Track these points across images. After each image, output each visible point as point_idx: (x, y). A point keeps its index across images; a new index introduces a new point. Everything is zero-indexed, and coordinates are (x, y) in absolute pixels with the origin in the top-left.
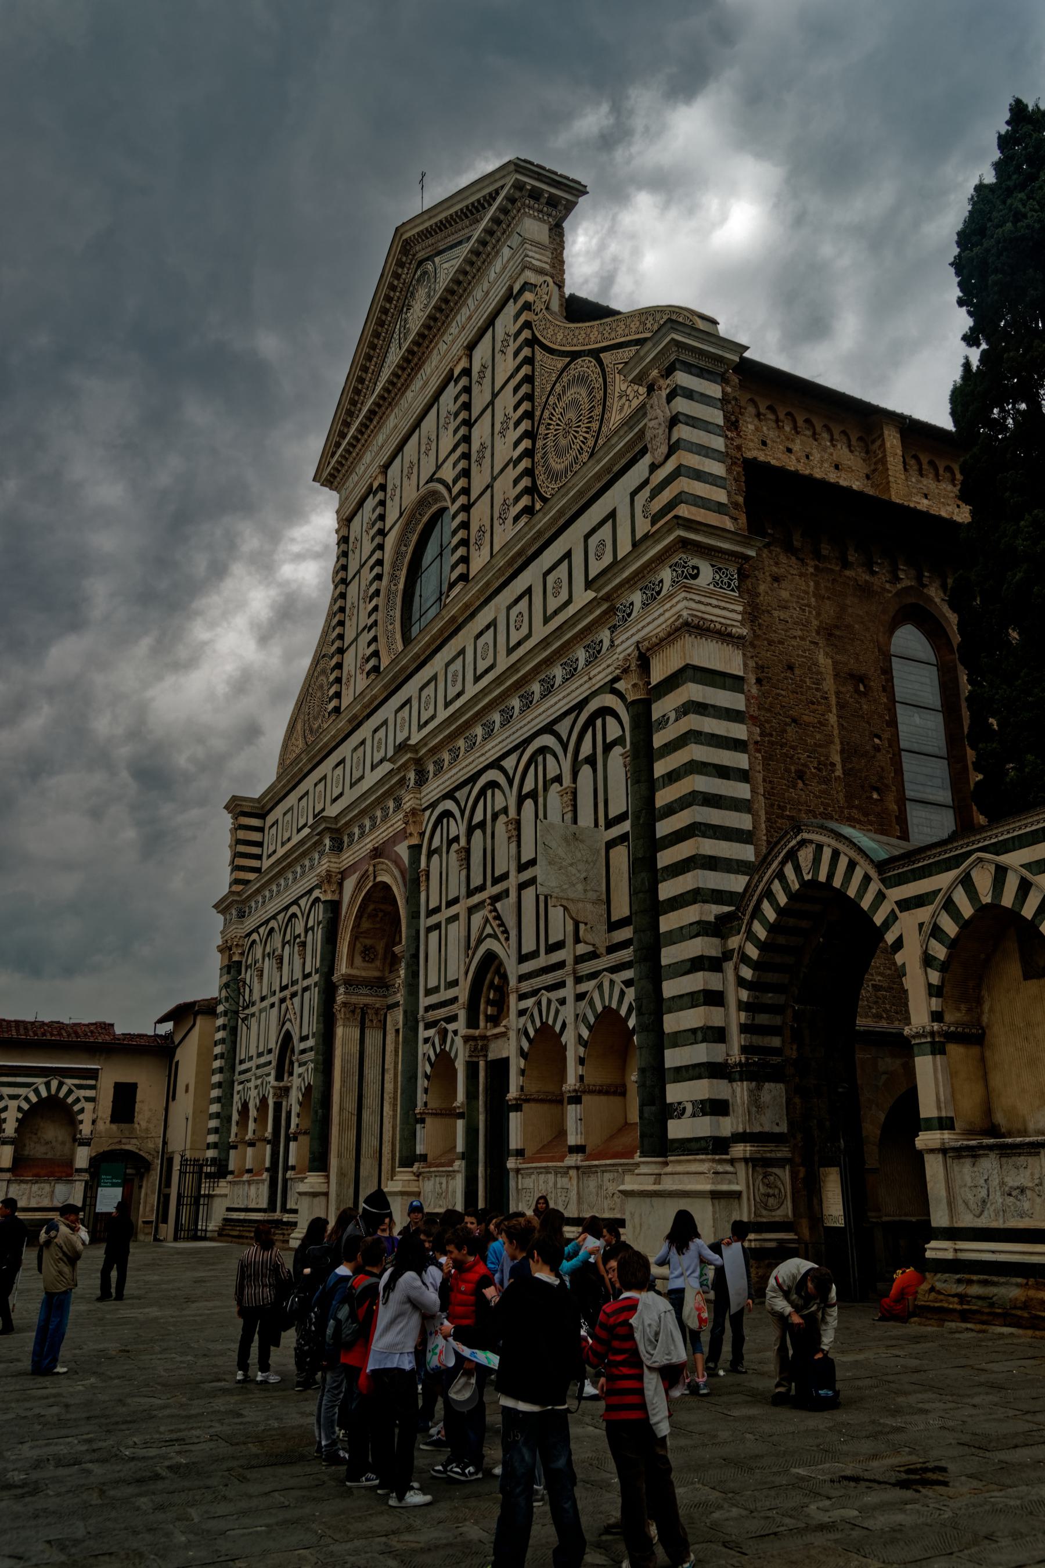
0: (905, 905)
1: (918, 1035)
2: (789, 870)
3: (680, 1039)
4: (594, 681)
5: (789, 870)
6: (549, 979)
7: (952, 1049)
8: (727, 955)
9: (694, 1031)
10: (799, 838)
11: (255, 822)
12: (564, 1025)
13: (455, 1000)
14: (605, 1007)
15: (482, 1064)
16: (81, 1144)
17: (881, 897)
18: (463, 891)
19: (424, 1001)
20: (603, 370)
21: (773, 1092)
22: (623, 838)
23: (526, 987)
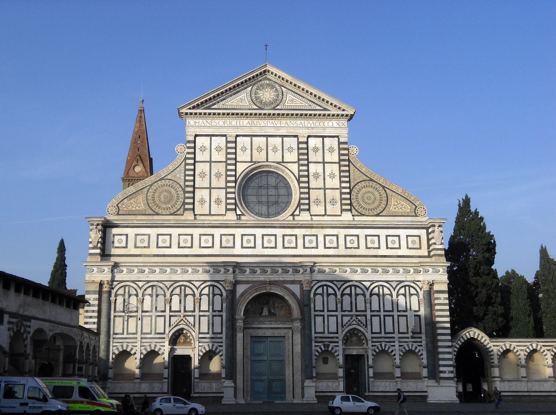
0: (494, 346)
2: (467, 334)
3: (443, 359)
13: (337, 338)
14: (409, 349)
16: (90, 365)
17: (488, 343)
18: (339, 309)
19: (314, 335)
20: (386, 193)
23: (374, 340)
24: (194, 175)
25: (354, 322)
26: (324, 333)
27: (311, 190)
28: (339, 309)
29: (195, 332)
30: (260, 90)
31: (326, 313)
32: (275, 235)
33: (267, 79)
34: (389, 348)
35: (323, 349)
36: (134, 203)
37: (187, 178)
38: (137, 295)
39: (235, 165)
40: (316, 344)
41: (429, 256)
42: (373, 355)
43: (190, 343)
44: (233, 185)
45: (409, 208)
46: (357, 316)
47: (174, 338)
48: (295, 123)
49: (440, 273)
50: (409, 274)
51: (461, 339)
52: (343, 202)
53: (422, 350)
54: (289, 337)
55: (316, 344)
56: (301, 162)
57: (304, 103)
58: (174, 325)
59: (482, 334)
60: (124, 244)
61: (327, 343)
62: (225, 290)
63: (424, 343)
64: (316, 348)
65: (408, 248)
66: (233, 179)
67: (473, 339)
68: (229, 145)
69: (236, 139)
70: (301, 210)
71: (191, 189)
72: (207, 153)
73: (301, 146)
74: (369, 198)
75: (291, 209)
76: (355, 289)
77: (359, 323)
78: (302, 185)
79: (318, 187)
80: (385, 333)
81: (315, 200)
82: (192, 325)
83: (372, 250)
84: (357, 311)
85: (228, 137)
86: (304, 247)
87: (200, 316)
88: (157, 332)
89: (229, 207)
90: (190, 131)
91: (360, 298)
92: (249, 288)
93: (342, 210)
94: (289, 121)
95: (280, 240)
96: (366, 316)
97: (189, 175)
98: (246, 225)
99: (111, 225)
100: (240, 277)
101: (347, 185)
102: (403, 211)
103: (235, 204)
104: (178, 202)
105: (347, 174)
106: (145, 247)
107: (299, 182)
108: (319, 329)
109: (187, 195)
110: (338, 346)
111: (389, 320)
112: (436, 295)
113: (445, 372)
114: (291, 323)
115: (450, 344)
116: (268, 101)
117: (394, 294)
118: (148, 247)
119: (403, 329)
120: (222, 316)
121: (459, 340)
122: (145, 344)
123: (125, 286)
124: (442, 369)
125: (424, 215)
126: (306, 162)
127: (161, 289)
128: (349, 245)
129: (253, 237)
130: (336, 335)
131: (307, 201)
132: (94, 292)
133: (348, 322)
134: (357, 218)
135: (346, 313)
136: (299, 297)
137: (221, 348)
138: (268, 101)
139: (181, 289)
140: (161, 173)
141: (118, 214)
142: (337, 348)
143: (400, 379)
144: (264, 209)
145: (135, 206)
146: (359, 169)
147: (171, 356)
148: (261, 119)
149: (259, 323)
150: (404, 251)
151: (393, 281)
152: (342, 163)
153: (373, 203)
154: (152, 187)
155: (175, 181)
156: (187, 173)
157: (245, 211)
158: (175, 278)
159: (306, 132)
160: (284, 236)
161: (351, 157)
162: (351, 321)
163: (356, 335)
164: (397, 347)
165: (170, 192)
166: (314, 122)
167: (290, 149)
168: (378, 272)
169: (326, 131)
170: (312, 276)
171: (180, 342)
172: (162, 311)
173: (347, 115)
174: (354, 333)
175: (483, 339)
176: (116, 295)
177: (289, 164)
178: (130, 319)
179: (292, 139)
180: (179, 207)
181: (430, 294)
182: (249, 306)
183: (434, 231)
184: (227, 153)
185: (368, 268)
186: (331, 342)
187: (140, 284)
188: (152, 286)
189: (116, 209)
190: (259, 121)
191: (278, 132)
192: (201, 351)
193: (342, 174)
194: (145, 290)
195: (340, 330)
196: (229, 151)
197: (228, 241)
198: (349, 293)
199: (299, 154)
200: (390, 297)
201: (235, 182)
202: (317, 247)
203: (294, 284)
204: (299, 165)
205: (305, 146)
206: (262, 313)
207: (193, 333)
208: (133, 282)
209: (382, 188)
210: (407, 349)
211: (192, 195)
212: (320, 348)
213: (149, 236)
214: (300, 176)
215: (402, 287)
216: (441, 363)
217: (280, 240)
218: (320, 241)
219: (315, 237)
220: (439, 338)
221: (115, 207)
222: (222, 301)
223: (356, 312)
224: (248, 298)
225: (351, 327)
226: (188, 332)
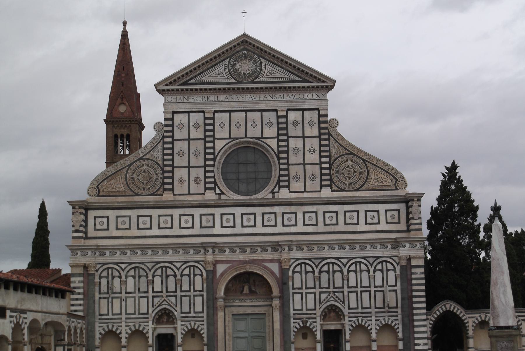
0: (469, 317)
1: (470, 336)
2: (443, 307)
4: (385, 254)
5: (443, 307)
6: (364, 315)
8: (427, 319)
10: (447, 303)
11: (84, 211)
13: (315, 314)
15: (322, 330)
17: (464, 315)
18: (317, 286)
19: (292, 312)
22: (394, 291)
23: (351, 315)
24: (172, 154)
25: (332, 299)
26: (302, 310)
27: (291, 167)
28: (317, 286)
29: (177, 312)
30: (238, 62)
31: (304, 291)
32: (255, 214)
33: (245, 49)
34: (366, 323)
35: (302, 325)
36: (113, 184)
37: (166, 157)
38: (120, 277)
39: (214, 142)
40: (295, 321)
41: (408, 231)
42: (350, 330)
43: (173, 323)
44: (212, 163)
45: (390, 181)
46: (334, 292)
48: (273, 96)
49: (417, 248)
50: (386, 249)
52: (323, 177)
53: (398, 324)
54: (269, 315)
55: (295, 321)
56: (281, 137)
57: (283, 74)
58: (157, 305)
59: (458, 307)
60: (105, 226)
61: (305, 319)
62: (206, 270)
63: (400, 317)
64: (294, 325)
65: (387, 223)
66: (212, 157)
67: (448, 312)
68: (207, 122)
69: (214, 114)
70: (280, 187)
71: (170, 169)
72: (185, 130)
73: (280, 120)
74: (349, 172)
75: (270, 186)
76: (333, 266)
77: (337, 299)
78: (281, 161)
79: (298, 163)
80: (362, 308)
81: (294, 177)
82: (174, 305)
83: (351, 226)
84: (334, 287)
85: (206, 114)
86: (284, 225)
87: (182, 296)
88: (141, 312)
89: (208, 186)
90: (167, 108)
91: (338, 275)
92: (229, 268)
93: (322, 186)
94: (268, 94)
95: (259, 219)
96: (343, 292)
97: (167, 154)
98: (225, 204)
99: (92, 207)
100: (220, 257)
101: (327, 160)
102: (384, 185)
104: (157, 182)
105: (327, 148)
106: (126, 229)
107: (279, 158)
108: (298, 306)
109: (166, 175)
110: (316, 322)
111: (366, 296)
112: (413, 270)
113: (419, 344)
114: (271, 300)
115: (425, 317)
116: (246, 73)
117: (372, 270)
118: (130, 228)
119: (379, 304)
120: (202, 296)
121: (435, 313)
122: (130, 324)
123: (108, 268)
124: (417, 341)
126: (285, 137)
127: (143, 271)
128: (328, 222)
129: (232, 216)
130: (314, 312)
131: (286, 178)
132: (79, 275)
133: (326, 299)
134: (336, 194)
135: (324, 290)
136: (278, 275)
137: (202, 326)
138: (246, 73)
139: (162, 270)
140: (140, 152)
141: (98, 196)
142: (315, 324)
144: (243, 187)
145: (115, 187)
146: (340, 142)
147: (155, 334)
148: (239, 93)
149: (241, 301)
150: (383, 226)
152: (323, 137)
153: (354, 177)
154: (131, 167)
155: (153, 161)
156: (166, 152)
157: (225, 189)
158: (156, 259)
159: (285, 106)
160: (263, 214)
161: (332, 130)
162: (329, 297)
163: (334, 311)
164: (374, 322)
165: (149, 172)
166: (294, 94)
167: (270, 124)
168: (355, 249)
169: (306, 103)
170: (290, 254)
171: (163, 321)
172: (145, 292)
173: (327, 87)
174: (332, 309)
175: (459, 311)
176: (100, 278)
177: (269, 140)
178: (115, 300)
179: (271, 113)
180: (158, 187)
182: (230, 285)
183: (412, 205)
184: (205, 130)
185: (345, 246)
186: (309, 318)
187: (123, 266)
188: (134, 268)
189: (96, 190)
190: (238, 95)
191: (256, 106)
192: (184, 330)
193: (322, 149)
194: (128, 272)
195: (318, 307)
196: (207, 127)
197: (207, 221)
198: (327, 270)
199: (279, 129)
200: (367, 273)
201: (214, 160)
202: (296, 225)
203: (273, 263)
204: (279, 141)
205: (284, 120)
206: (243, 291)
207: (175, 313)
208: (116, 264)
209: (362, 162)
210: (384, 323)
211: (170, 175)
212: (299, 324)
213: (130, 217)
214: (279, 152)
215: (379, 263)
216: (416, 335)
217: (259, 219)
218: (300, 219)
219: (294, 214)
220: (415, 311)
221: (95, 188)
222: (203, 281)
223: (333, 288)
224: (228, 277)
225: (329, 303)
226: (170, 312)
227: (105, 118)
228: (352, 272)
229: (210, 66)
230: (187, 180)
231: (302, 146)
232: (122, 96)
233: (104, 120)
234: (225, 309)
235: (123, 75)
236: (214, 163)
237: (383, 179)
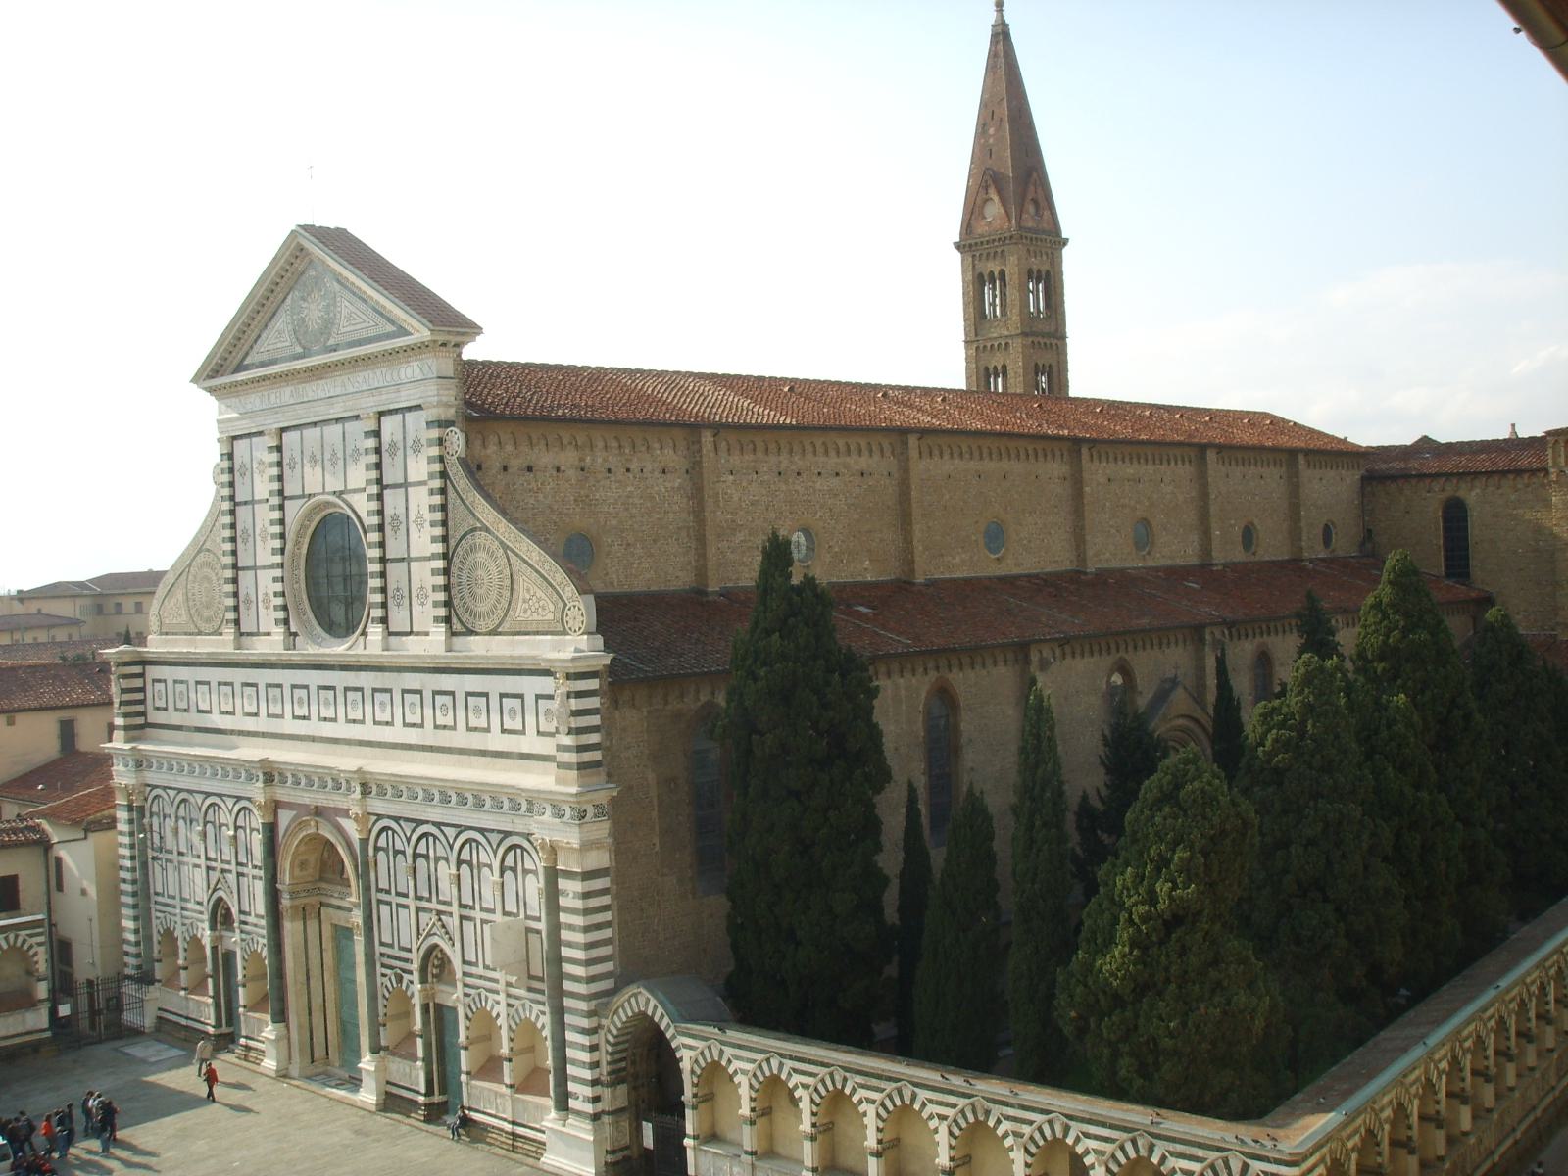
2: (633, 1000)
7: (701, 1106)
9: (584, 1063)
11: (137, 670)
12: (498, 1015)
16: (39, 980)
19: (379, 949)
21: (623, 1089)
26: (391, 946)
42: (467, 1017)
43: (234, 931)
47: (224, 912)
51: (621, 1010)
55: (385, 971)
61: (399, 971)
65: (538, 732)
66: (278, 544)
100: (282, 794)
103: (285, 608)
121: (616, 1012)
125: (580, 629)
143: (508, 1091)
151: (493, 831)
165: (207, 579)
166: (384, 370)
169: (402, 394)
176: (151, 816)
181: (552, 875)
191: (332, 411)
209: (501, 550)
227: (958, 240)
228: (464, 865)
229: (267, 316)
230: (254, 599)
231: (404, 510)
232: (986, 182)
233: (955, 244)
234: (320, 909)
235: (991, 131)
236: (283, 559)
237: (539, 599)
